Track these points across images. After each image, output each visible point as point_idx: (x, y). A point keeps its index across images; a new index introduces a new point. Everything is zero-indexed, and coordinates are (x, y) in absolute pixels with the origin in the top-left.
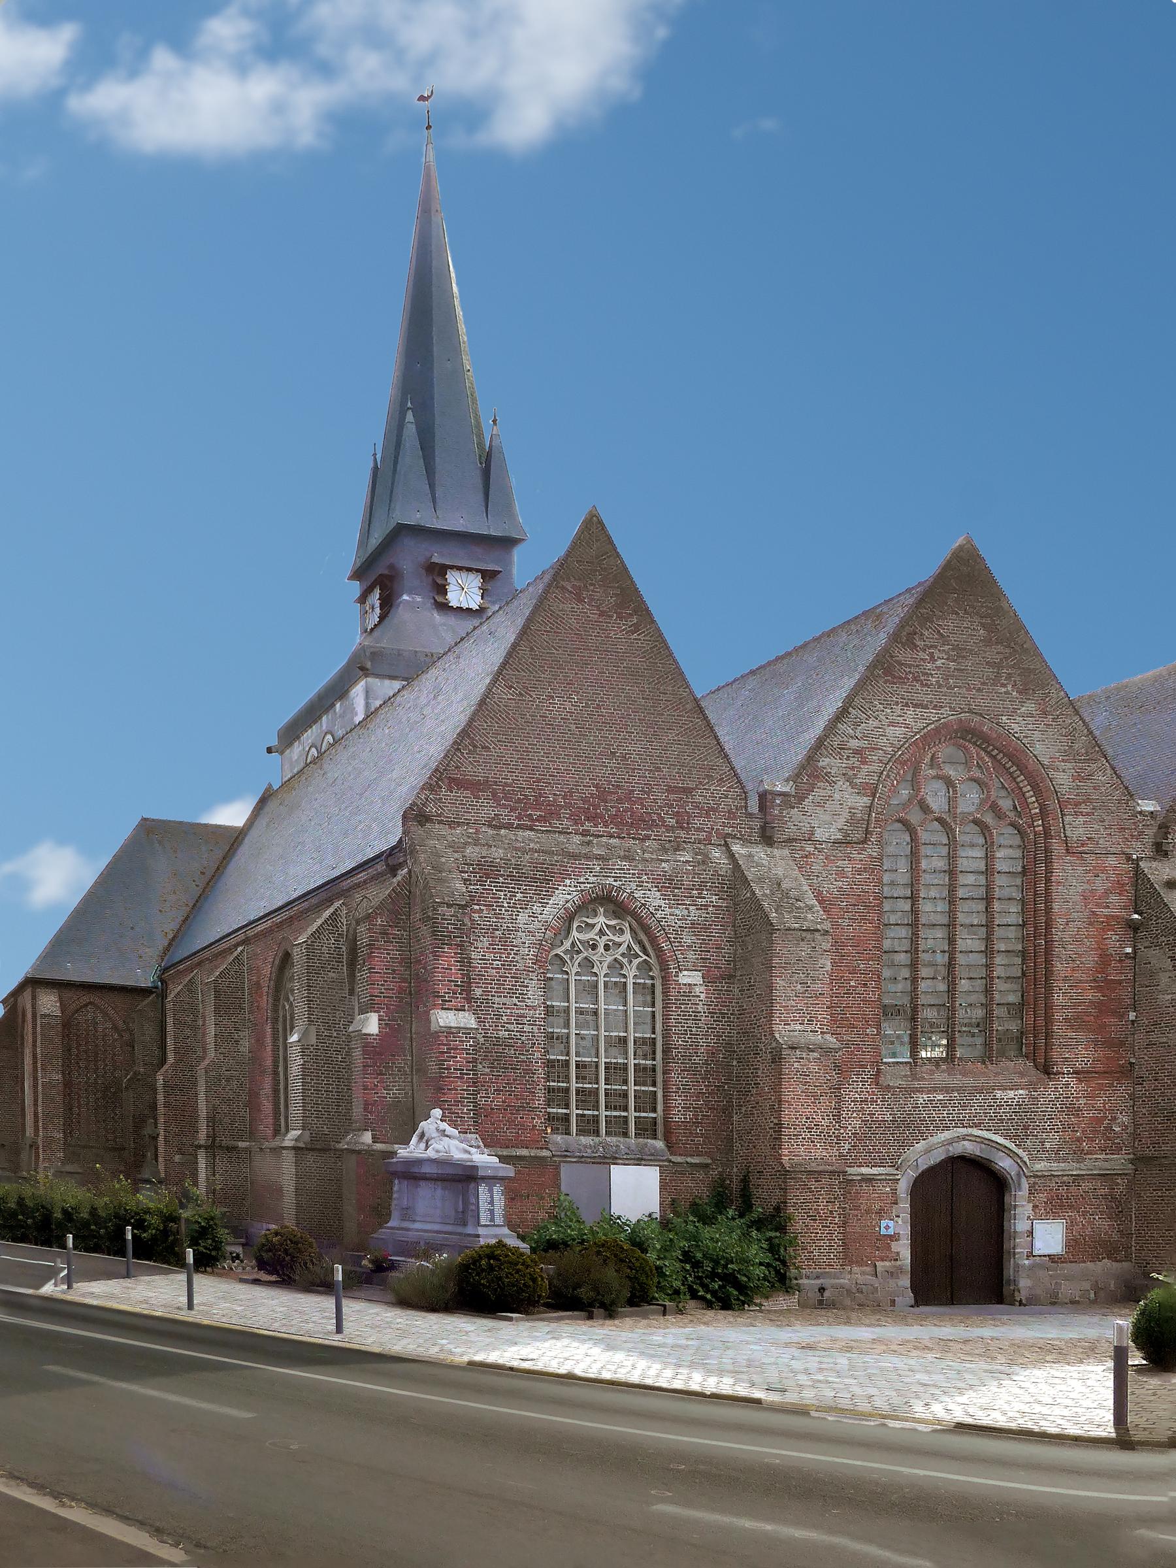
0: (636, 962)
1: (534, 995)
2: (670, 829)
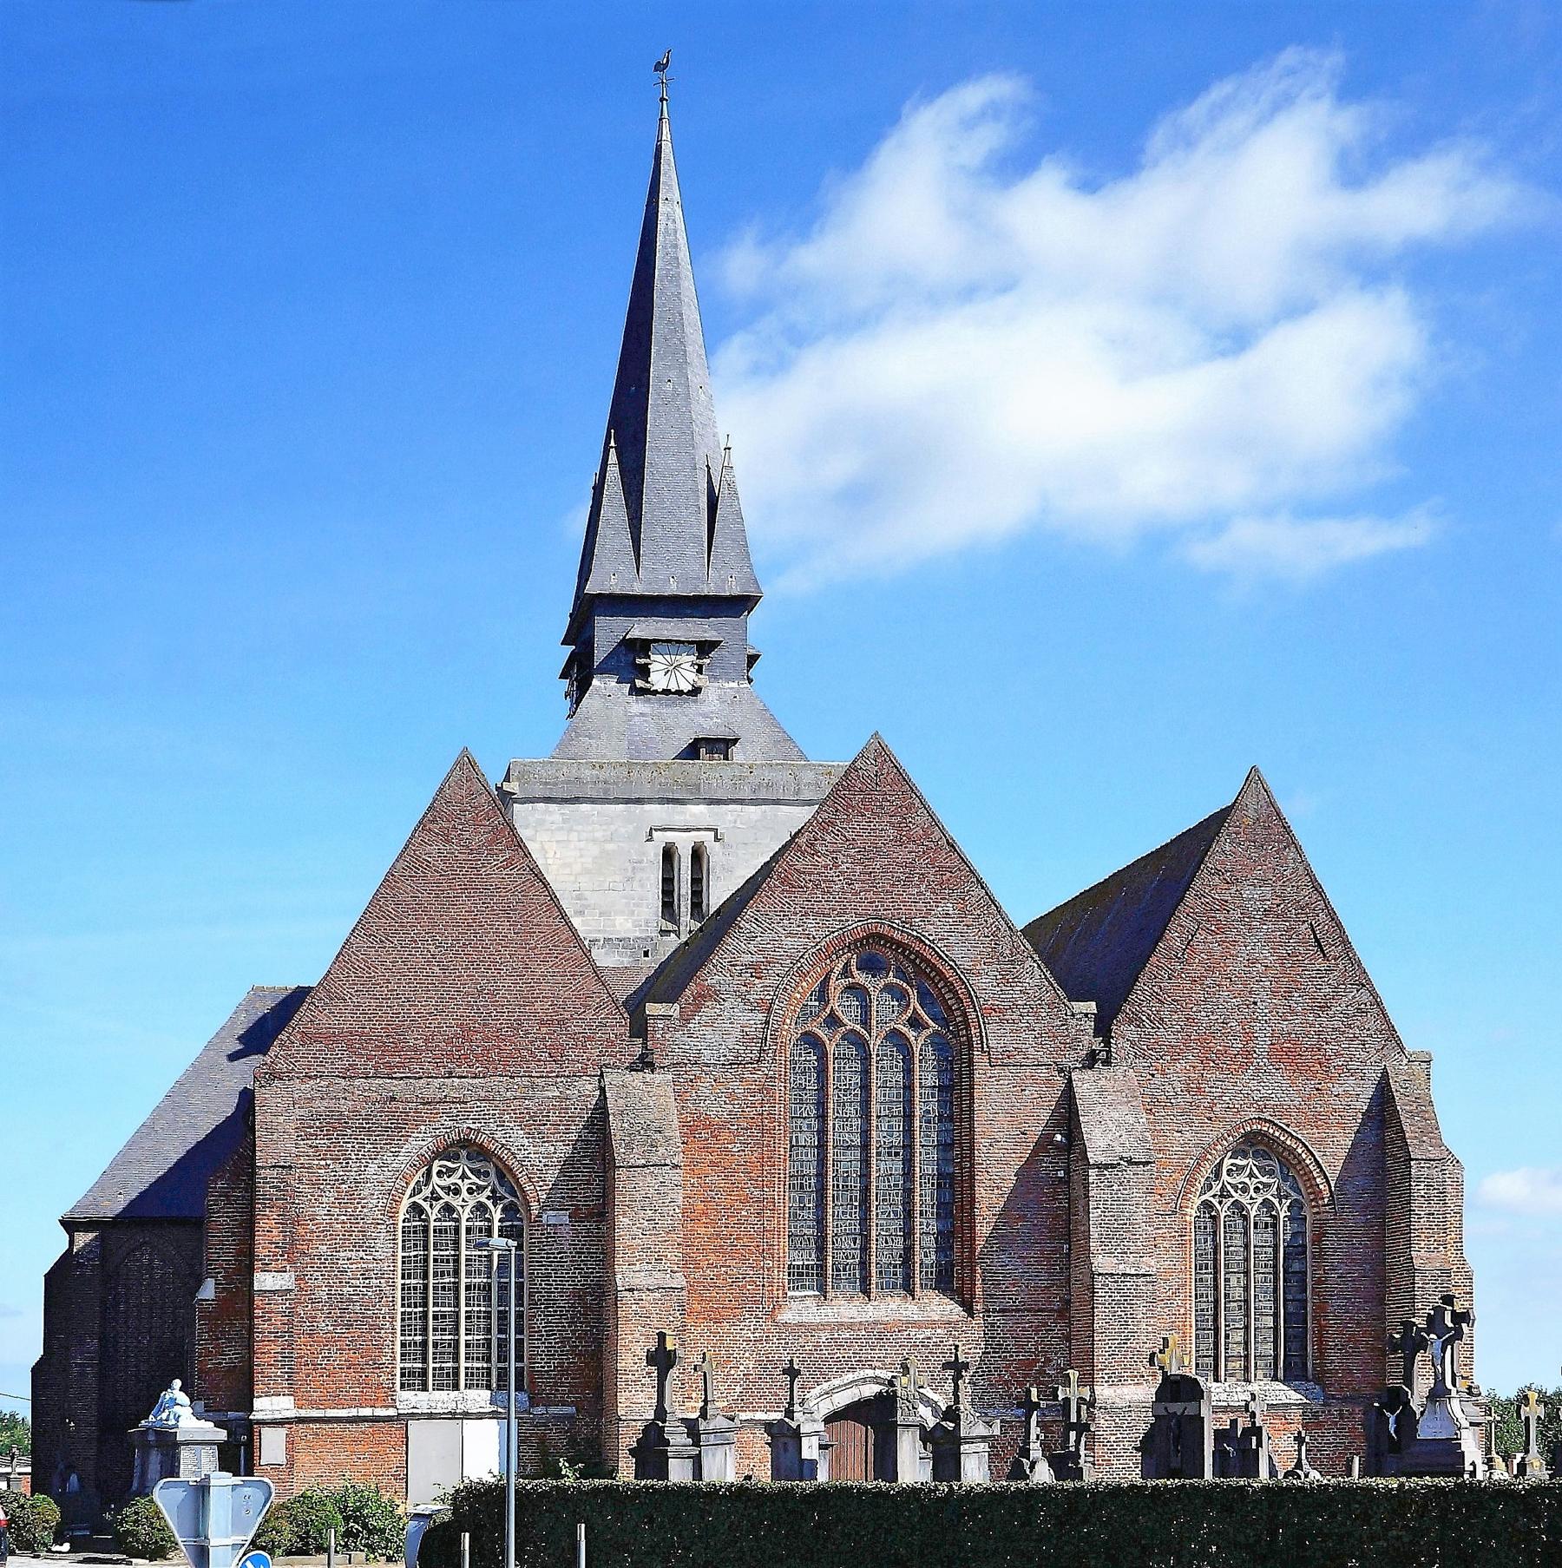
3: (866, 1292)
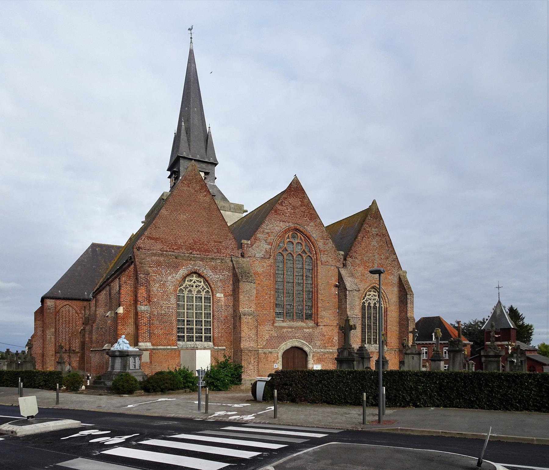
0: (205, 291)
1: (173, 300)
2: (215, 253)
3: (293, 319)
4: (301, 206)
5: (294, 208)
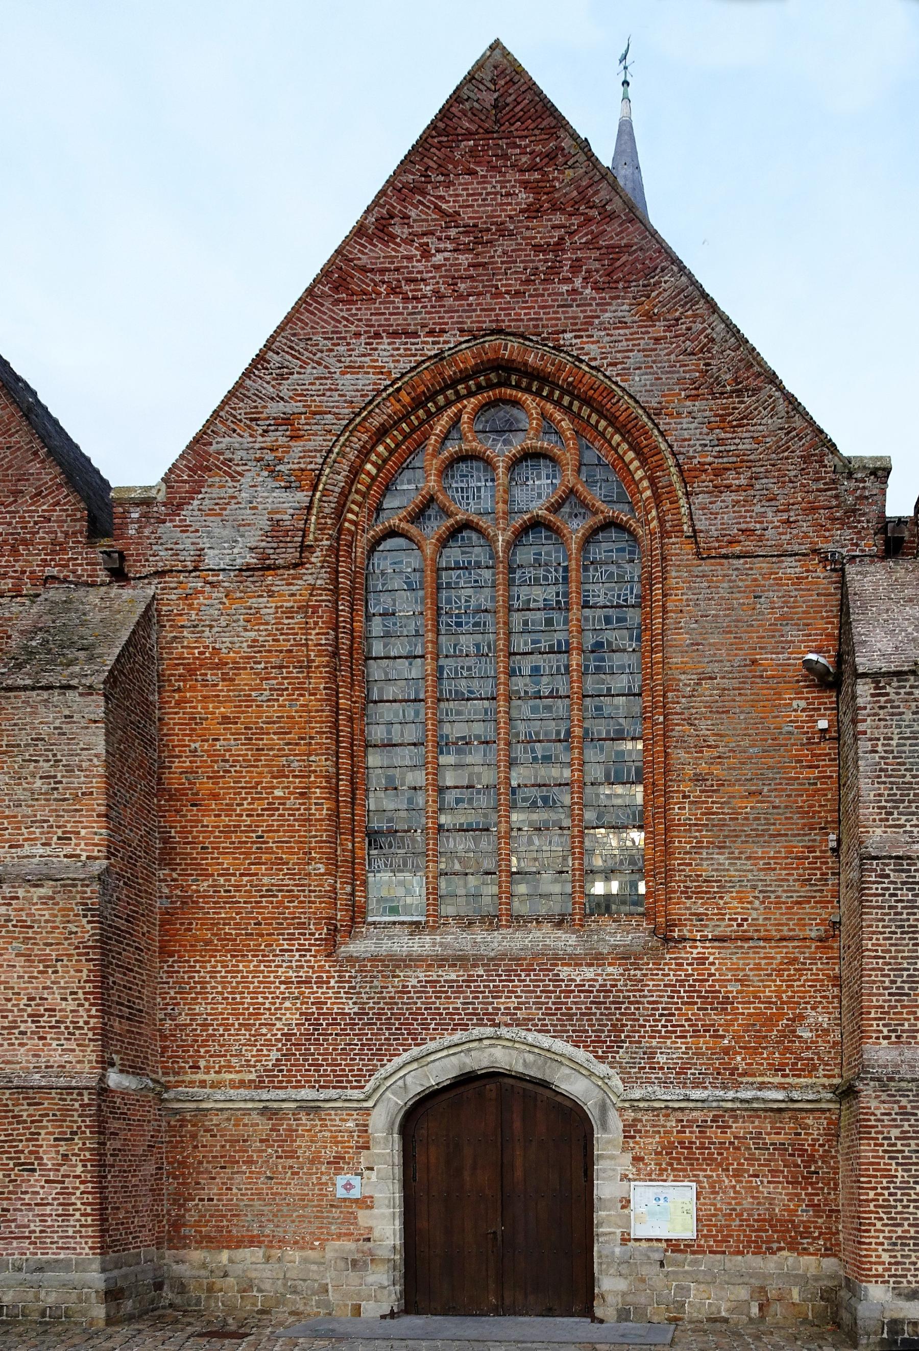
4: (533, 212)
5: (477, 237)
